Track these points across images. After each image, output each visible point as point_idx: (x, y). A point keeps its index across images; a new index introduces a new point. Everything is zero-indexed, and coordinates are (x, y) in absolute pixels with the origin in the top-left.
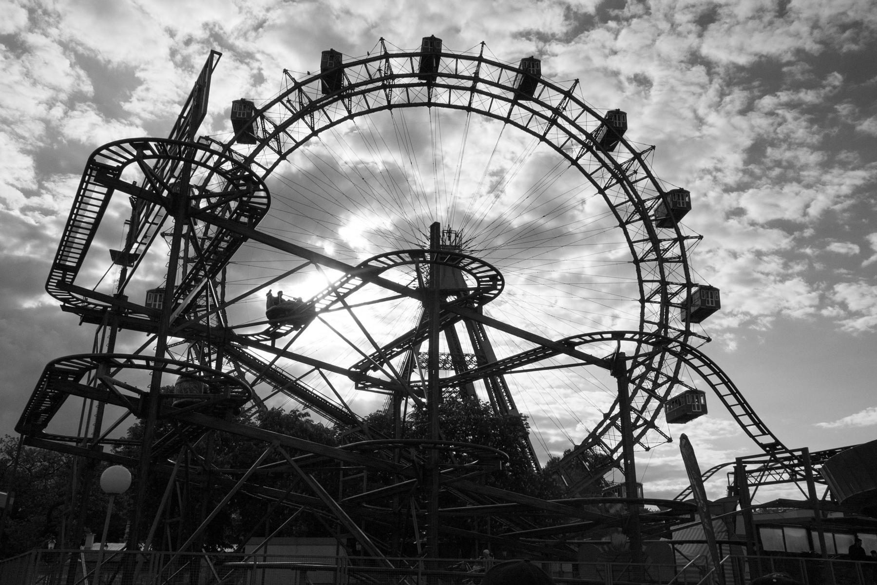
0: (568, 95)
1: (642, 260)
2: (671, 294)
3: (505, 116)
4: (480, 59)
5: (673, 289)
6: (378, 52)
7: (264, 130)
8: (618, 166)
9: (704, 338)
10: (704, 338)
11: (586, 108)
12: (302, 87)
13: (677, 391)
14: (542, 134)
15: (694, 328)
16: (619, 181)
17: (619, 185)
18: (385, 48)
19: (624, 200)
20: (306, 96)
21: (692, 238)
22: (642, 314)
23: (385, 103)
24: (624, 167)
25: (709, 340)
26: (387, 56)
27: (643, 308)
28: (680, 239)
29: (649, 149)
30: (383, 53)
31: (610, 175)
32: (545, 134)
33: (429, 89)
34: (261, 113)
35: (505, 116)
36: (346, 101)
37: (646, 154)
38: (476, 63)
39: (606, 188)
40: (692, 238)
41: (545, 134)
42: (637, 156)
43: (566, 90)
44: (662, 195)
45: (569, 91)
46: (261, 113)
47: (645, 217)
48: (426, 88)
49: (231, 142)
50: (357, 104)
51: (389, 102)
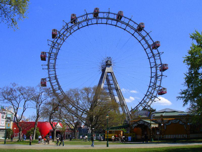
0: (148, 34)
1: (153, 77)
3: (133, 34)
4: (130, 20)
9: (159, 99)
10: (159, 99)
15: (158, 96)
21: (165, 76)
22: (148, 89)
25: (160, 100)
27: (149, 88)
33: (117, 22)
35: (133, 34)
40: (165, 76)
42: (159, 53)
44: (161, 64)
47: (156, 67)
50: (100, 21)
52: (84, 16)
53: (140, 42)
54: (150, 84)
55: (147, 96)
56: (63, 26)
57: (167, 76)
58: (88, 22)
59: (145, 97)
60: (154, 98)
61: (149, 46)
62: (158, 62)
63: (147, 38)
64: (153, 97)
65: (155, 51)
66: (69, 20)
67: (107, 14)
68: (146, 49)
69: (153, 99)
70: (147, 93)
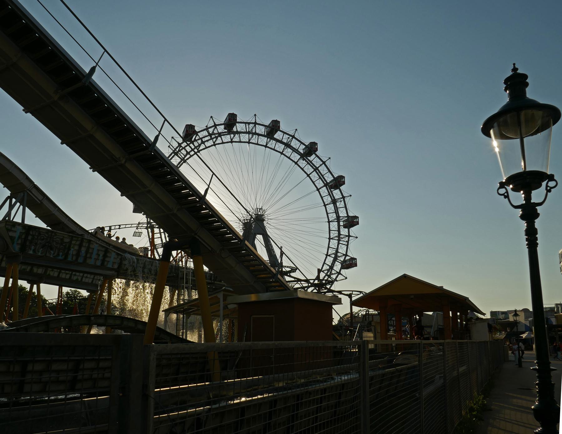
0: (343, 197)
4: (324, 163)
6: (291, 133)
11: (346, 207)
12: (257, 125)
14: (326, 204)
18: (295, 134)
23: (281, 151)
26: (293, 137)
29: (355, 237)
30: (293, 135)
32: (327, 204)
35: (319, 188)
36: (269, 139)
38: (322, 163)
39: (332, 239)
41: (327, 204)
42: (349, 236)
43: (344, 196)
45: (345, 197)
48: (300, 156)
50: (272, 144)
51: (283, 151)
52: (249, 123)
53: (325, 205)
56: (207, 126)
58: (252, 137)
61: (338, 218)
62: (342, 250)
63: (340, 204)
65: (344, 231)
66: (222, 119)
67: (289, 138)
68: (331, 221)
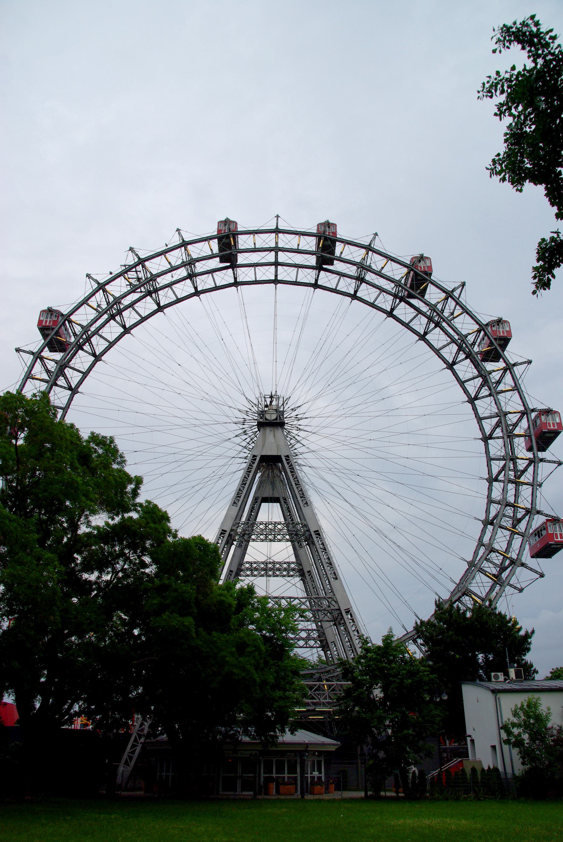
2: (511, 425)
5: (512, 419)
7: (75, 334)
8: (433, 308)
13: (538, 521)
16: (437, 325)
17: (438, 329)
19: (446, 343)
20: (110, 294)
21: (521, 364)
24: (439, 307)
28: (509, 368)
31: (426, 320)
34: (67, 318)
37: (458, 291)
40: (521, 364)
42: (449, 295)
44: (482, 328)
46: (67, 318)
49: (42, 350)
54: (482, 429)
55: (496, 480)
57: (530, 362)
59: (490, 489)
60: (531, 469)
64: (521, 467)
69: (527, 477)
70: (489, 466)
